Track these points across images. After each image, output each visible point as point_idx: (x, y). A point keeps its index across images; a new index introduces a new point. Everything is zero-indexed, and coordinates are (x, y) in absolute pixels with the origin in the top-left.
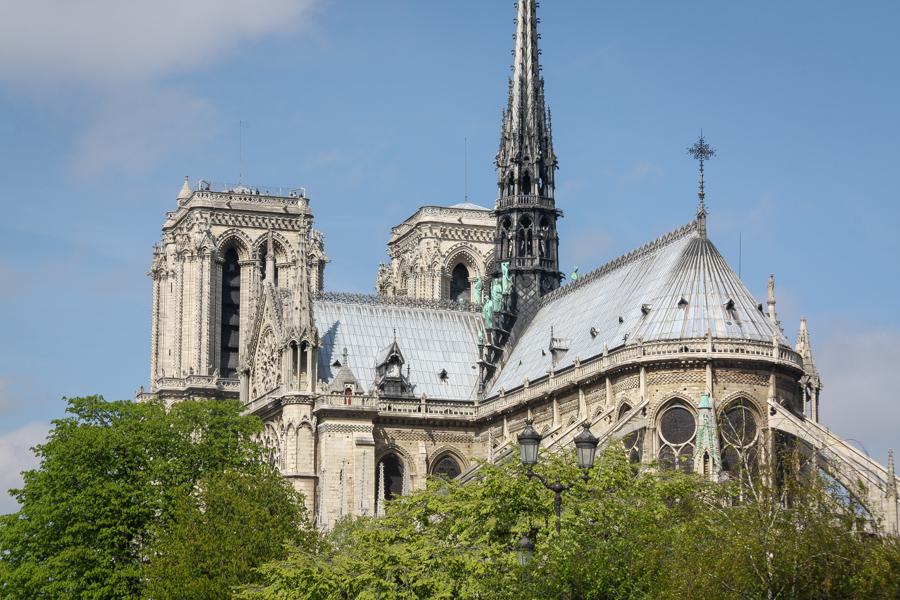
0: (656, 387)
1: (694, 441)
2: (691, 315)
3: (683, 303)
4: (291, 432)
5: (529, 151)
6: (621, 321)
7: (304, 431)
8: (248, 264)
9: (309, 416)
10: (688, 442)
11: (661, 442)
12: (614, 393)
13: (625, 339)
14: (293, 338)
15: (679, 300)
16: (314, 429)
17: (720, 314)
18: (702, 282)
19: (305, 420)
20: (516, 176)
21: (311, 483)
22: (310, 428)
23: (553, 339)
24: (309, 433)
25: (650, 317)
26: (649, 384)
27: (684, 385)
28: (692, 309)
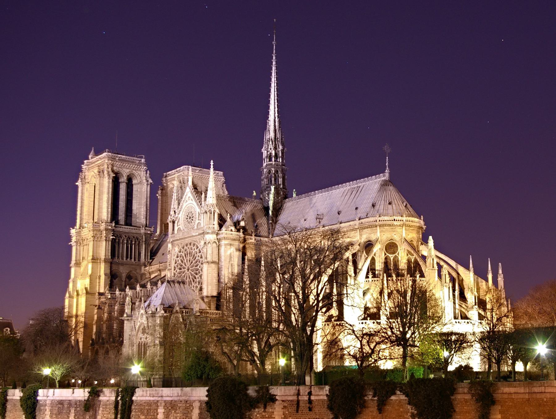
0: (383, 233)
1: (398, 254)
2: (394, 208)
3: (390, 203)
4: (209, 245)
5: (277, 146)
6: (356, 209)
7: (215, 244)
8: (123, 182)
9: (216, 239)
10: (396, 254)
11: (385, 254)
12: (361, 235)
13: (367, 215)
14: (210, 209)
15: (388, 202)
16: (218, 244)
17: (404, 208)
18: (394, 196)
19: (215, 241)
20: (274, 154)
21: (217, 266)
22: (217, 245)
23: (318, 215)
24: (216, 246)
25: (377, 207)
26: (380, 232)
27: (395, 233)
28: (394, 206)
